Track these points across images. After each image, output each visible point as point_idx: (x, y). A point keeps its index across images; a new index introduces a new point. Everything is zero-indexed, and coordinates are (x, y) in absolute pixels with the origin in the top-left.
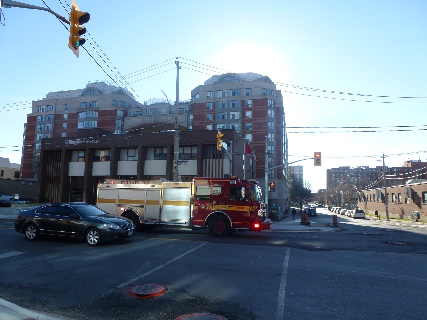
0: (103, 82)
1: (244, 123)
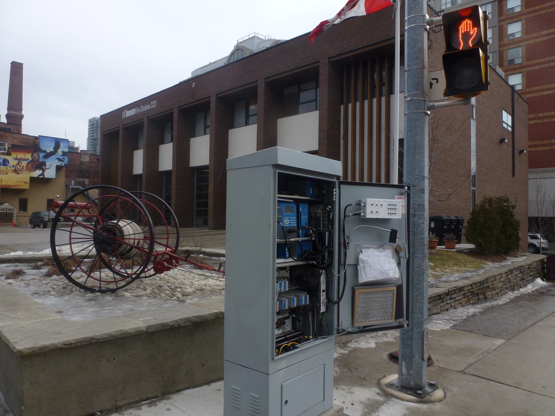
0: (256, 36)
1: (503, 51)
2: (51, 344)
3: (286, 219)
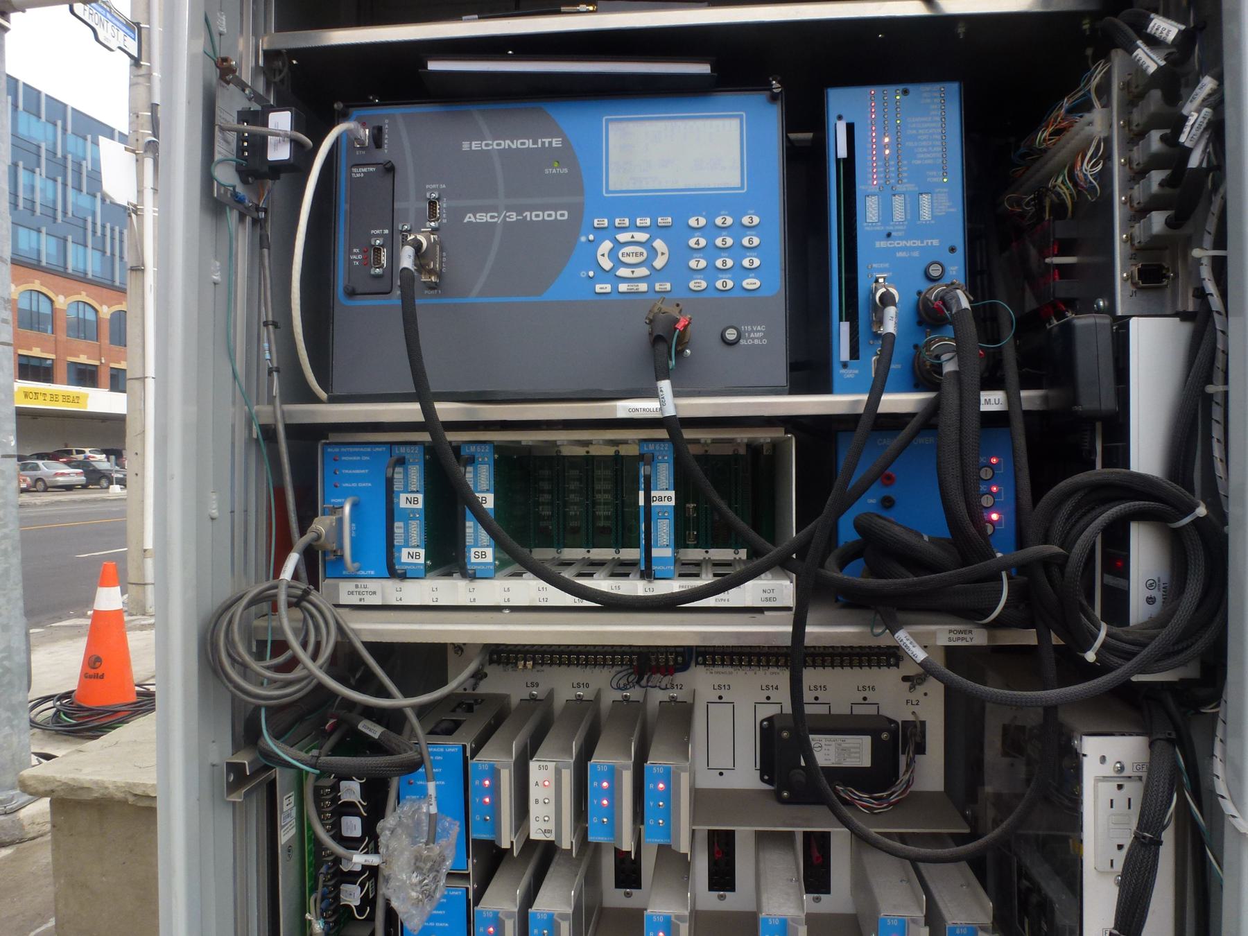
2: (96, 783)
3: (623, 237)
